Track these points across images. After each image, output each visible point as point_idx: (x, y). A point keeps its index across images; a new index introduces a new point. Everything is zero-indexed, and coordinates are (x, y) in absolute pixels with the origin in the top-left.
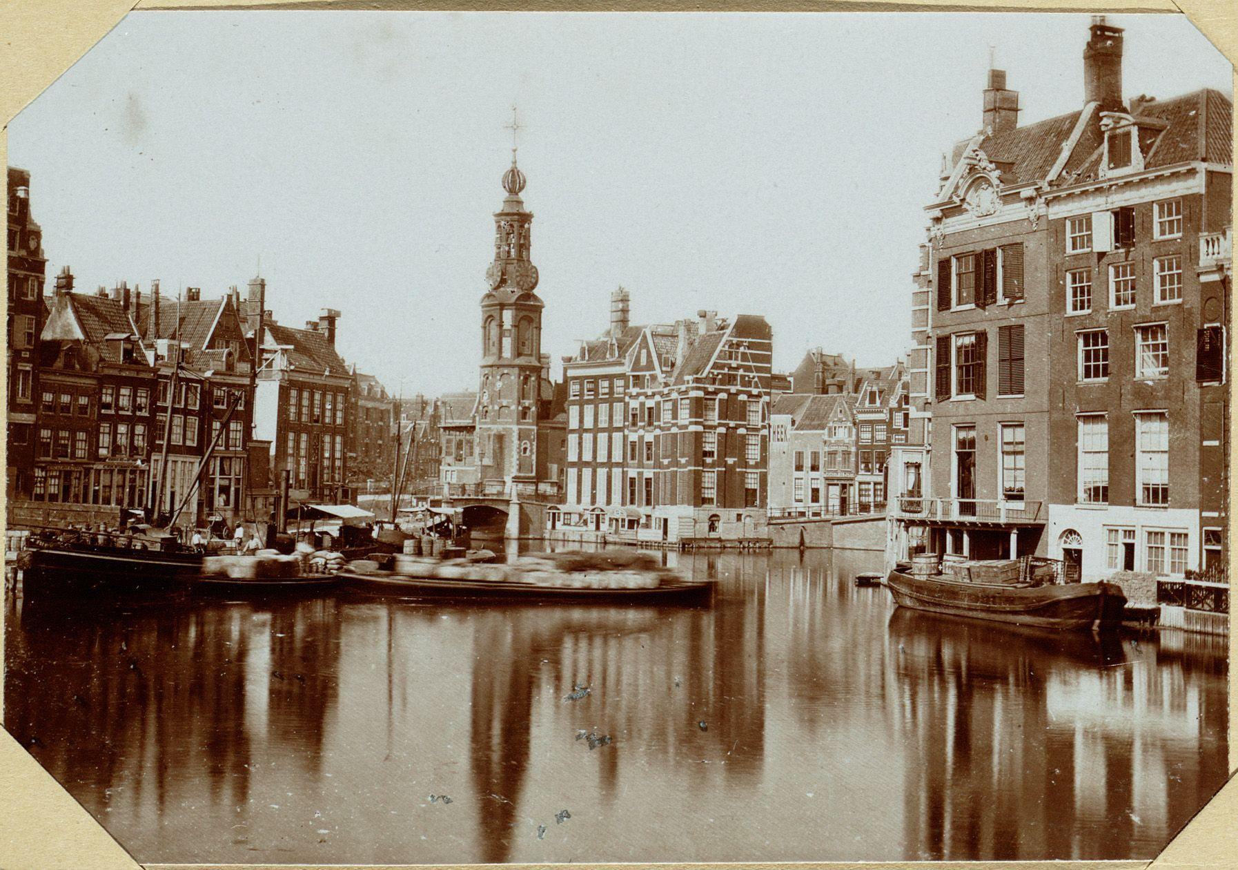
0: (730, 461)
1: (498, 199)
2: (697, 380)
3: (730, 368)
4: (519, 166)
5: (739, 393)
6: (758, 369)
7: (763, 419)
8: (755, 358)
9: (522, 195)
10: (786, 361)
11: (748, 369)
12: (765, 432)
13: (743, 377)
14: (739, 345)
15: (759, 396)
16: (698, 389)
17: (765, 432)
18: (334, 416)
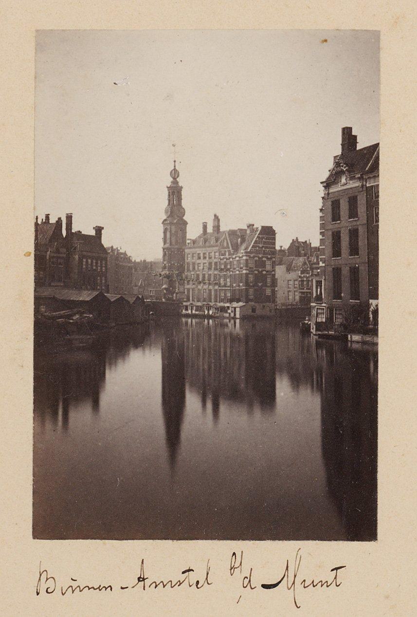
0: (260, 284)
1: (169, 181)
2: (246, 252)
3: (259, 247)
4: (177, 168)
5: (262, 257)
6: (271, 248)
7: (273, 268)
8: (268, 243)
9: (177, 179)
10: (283, 242)
11: (266, 247)
12: (273, 273)
13: (264, 251)
14: (263, 238)
15: (271, 258)
16: (246, 256)
17: (273, 273)
18: (101, 268)
